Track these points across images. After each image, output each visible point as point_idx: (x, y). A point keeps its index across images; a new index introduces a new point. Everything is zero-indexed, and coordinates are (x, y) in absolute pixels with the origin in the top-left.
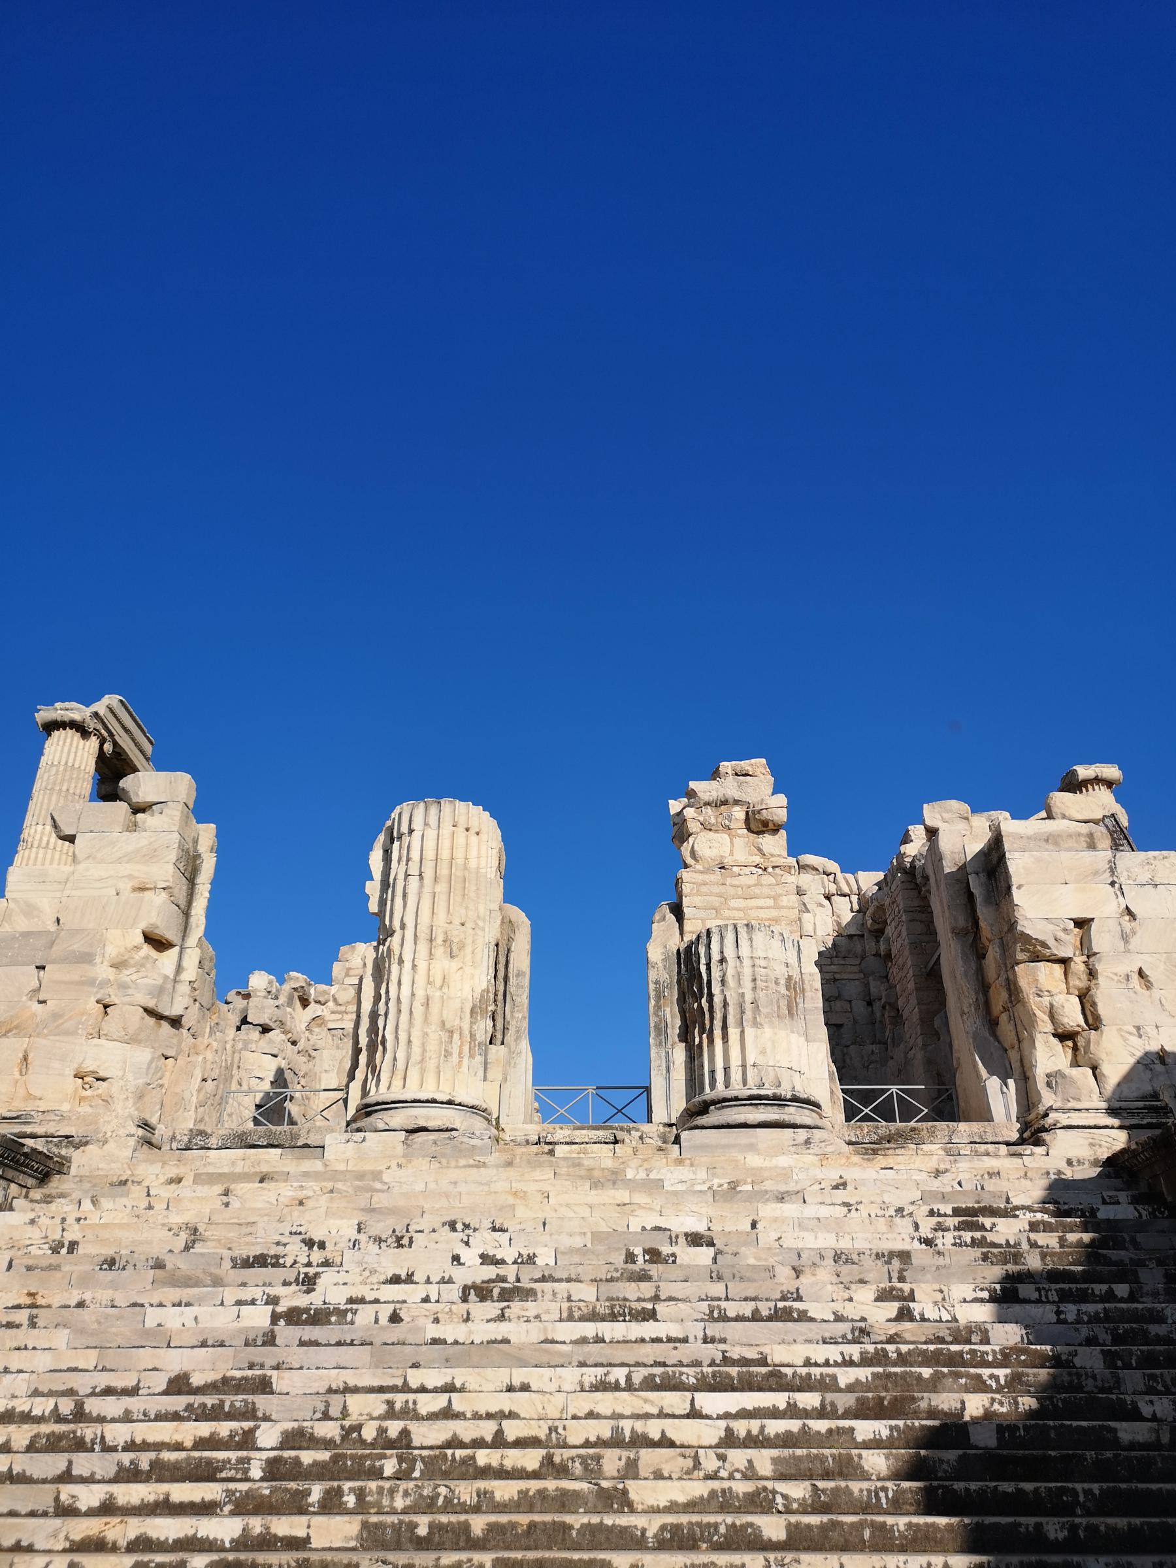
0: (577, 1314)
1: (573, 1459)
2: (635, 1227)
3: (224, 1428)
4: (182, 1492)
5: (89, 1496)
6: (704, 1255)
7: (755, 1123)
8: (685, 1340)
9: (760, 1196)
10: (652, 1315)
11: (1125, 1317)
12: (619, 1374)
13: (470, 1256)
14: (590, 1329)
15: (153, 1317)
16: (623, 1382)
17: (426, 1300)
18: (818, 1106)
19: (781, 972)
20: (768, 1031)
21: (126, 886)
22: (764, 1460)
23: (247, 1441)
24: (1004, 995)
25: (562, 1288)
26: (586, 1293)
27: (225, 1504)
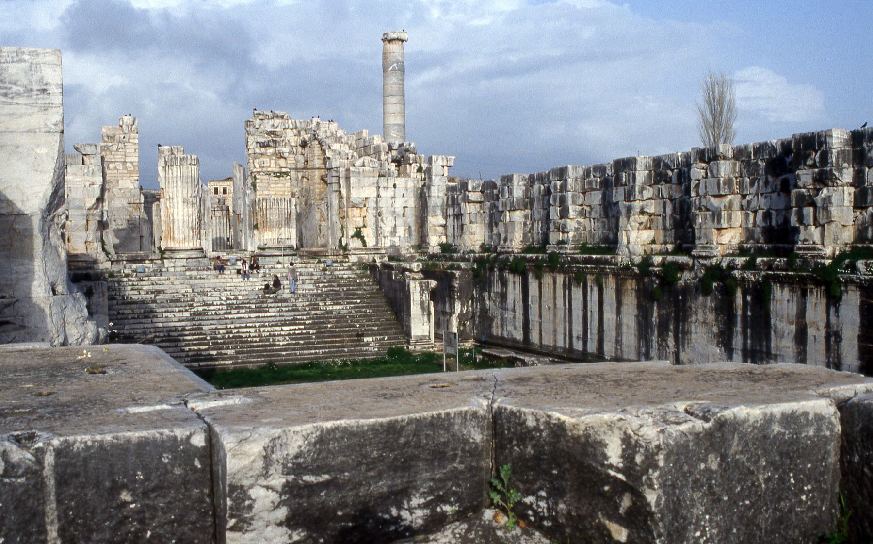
10: (266, 312)
14: (257, 315)
23: (205, 339)
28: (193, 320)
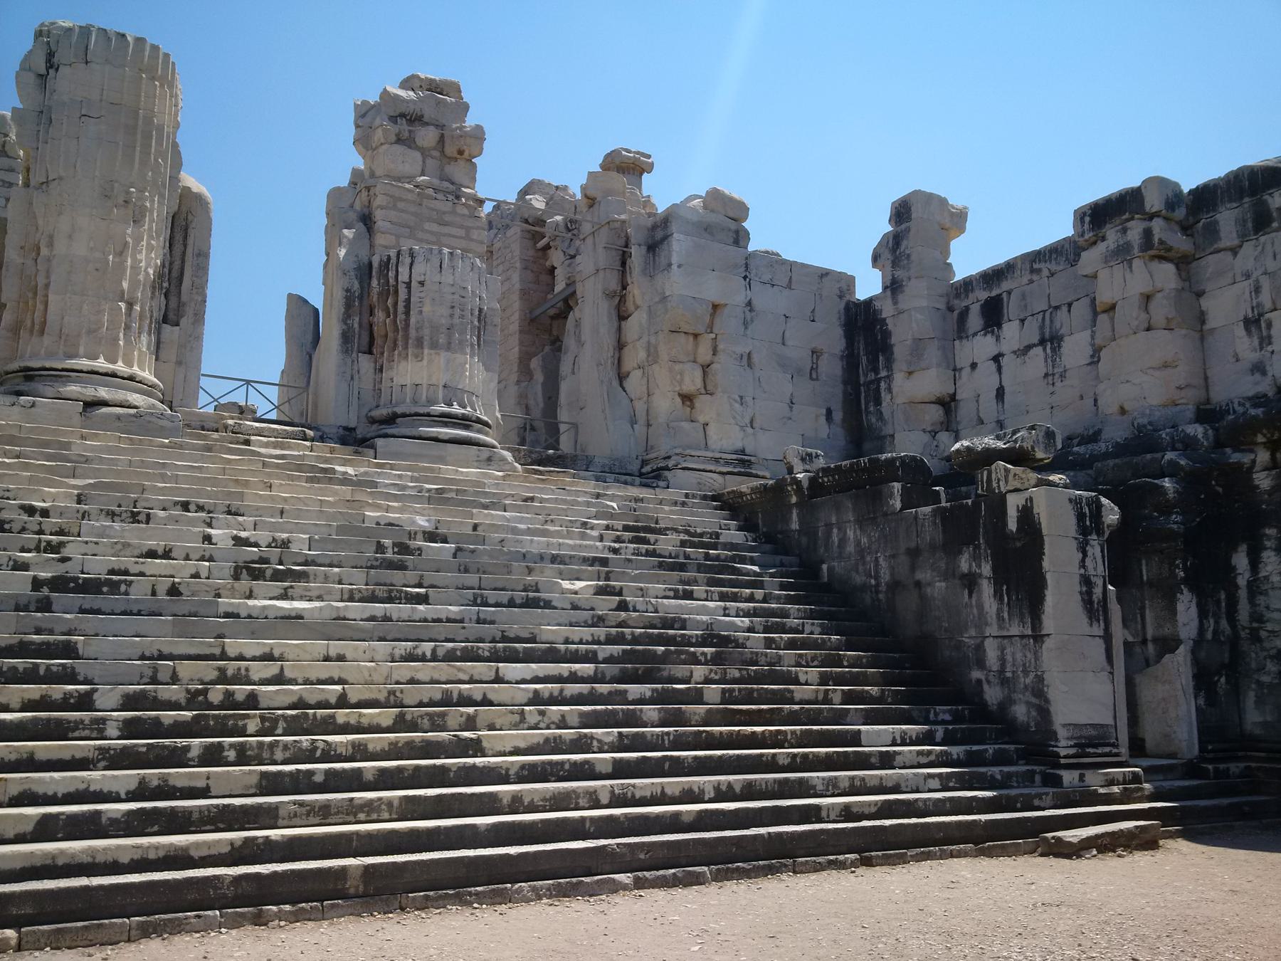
0: (357, 596)
1: (421, 717)
7: (446, 438)
8: (462, 621)
12: (427, 647)
14: (378, 608)
16: (428, 654)
17: (196, 576)
24: (642, 355)
27: (99, 761)
28: (45, 606)
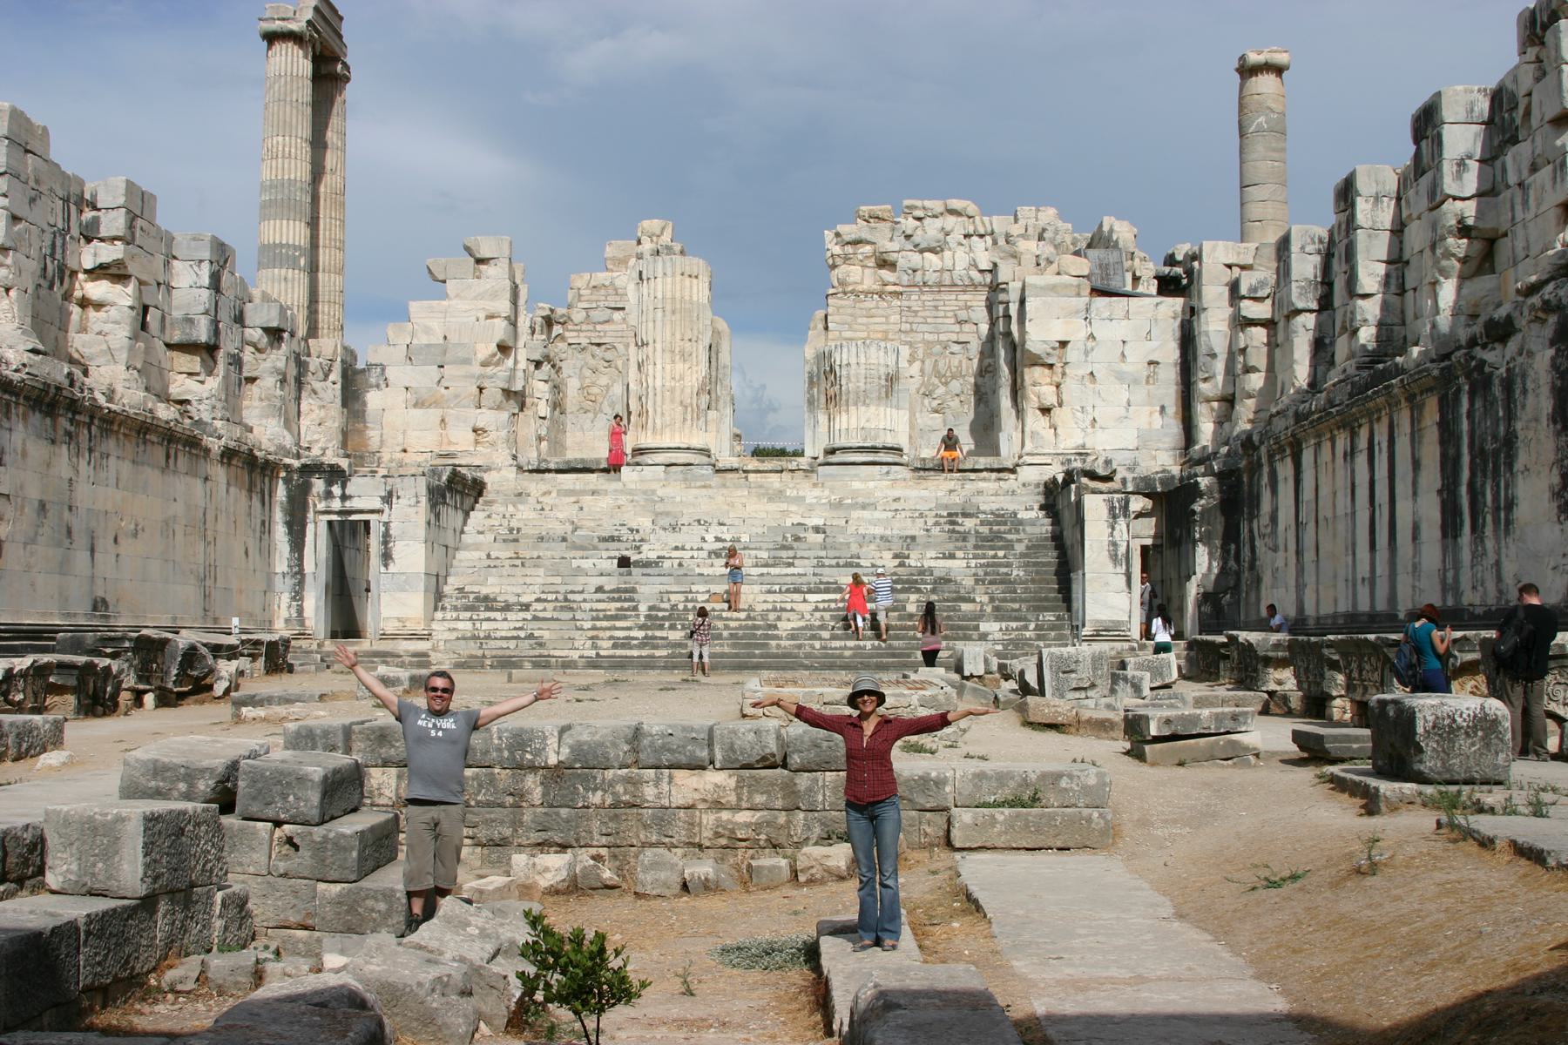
2: (788, 523)
3: (626, 605)
4: (619, 624)
5: (588, 625)
6: (820, 537)
9: (854, 506)
11: (994, 565)
12: (777, 588)
13: (710, 537)
14: (765, 570)
15: (575, 563)
18: (900, 450)
19: (883, 371)
20: (873, 408)
21: (482, 315)
22: (827, 615)
23: (635, 609)
25: (753, 553)
26: (765, 555)
